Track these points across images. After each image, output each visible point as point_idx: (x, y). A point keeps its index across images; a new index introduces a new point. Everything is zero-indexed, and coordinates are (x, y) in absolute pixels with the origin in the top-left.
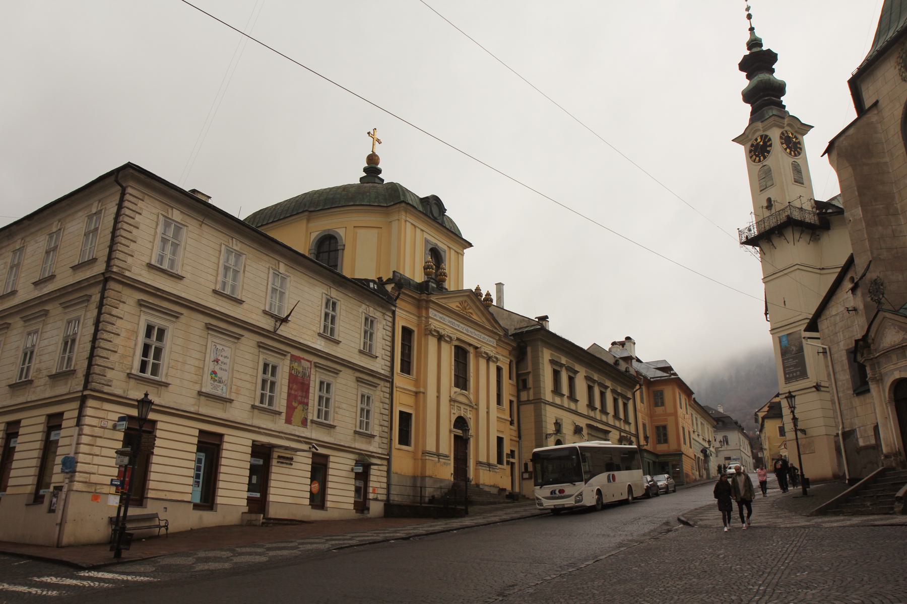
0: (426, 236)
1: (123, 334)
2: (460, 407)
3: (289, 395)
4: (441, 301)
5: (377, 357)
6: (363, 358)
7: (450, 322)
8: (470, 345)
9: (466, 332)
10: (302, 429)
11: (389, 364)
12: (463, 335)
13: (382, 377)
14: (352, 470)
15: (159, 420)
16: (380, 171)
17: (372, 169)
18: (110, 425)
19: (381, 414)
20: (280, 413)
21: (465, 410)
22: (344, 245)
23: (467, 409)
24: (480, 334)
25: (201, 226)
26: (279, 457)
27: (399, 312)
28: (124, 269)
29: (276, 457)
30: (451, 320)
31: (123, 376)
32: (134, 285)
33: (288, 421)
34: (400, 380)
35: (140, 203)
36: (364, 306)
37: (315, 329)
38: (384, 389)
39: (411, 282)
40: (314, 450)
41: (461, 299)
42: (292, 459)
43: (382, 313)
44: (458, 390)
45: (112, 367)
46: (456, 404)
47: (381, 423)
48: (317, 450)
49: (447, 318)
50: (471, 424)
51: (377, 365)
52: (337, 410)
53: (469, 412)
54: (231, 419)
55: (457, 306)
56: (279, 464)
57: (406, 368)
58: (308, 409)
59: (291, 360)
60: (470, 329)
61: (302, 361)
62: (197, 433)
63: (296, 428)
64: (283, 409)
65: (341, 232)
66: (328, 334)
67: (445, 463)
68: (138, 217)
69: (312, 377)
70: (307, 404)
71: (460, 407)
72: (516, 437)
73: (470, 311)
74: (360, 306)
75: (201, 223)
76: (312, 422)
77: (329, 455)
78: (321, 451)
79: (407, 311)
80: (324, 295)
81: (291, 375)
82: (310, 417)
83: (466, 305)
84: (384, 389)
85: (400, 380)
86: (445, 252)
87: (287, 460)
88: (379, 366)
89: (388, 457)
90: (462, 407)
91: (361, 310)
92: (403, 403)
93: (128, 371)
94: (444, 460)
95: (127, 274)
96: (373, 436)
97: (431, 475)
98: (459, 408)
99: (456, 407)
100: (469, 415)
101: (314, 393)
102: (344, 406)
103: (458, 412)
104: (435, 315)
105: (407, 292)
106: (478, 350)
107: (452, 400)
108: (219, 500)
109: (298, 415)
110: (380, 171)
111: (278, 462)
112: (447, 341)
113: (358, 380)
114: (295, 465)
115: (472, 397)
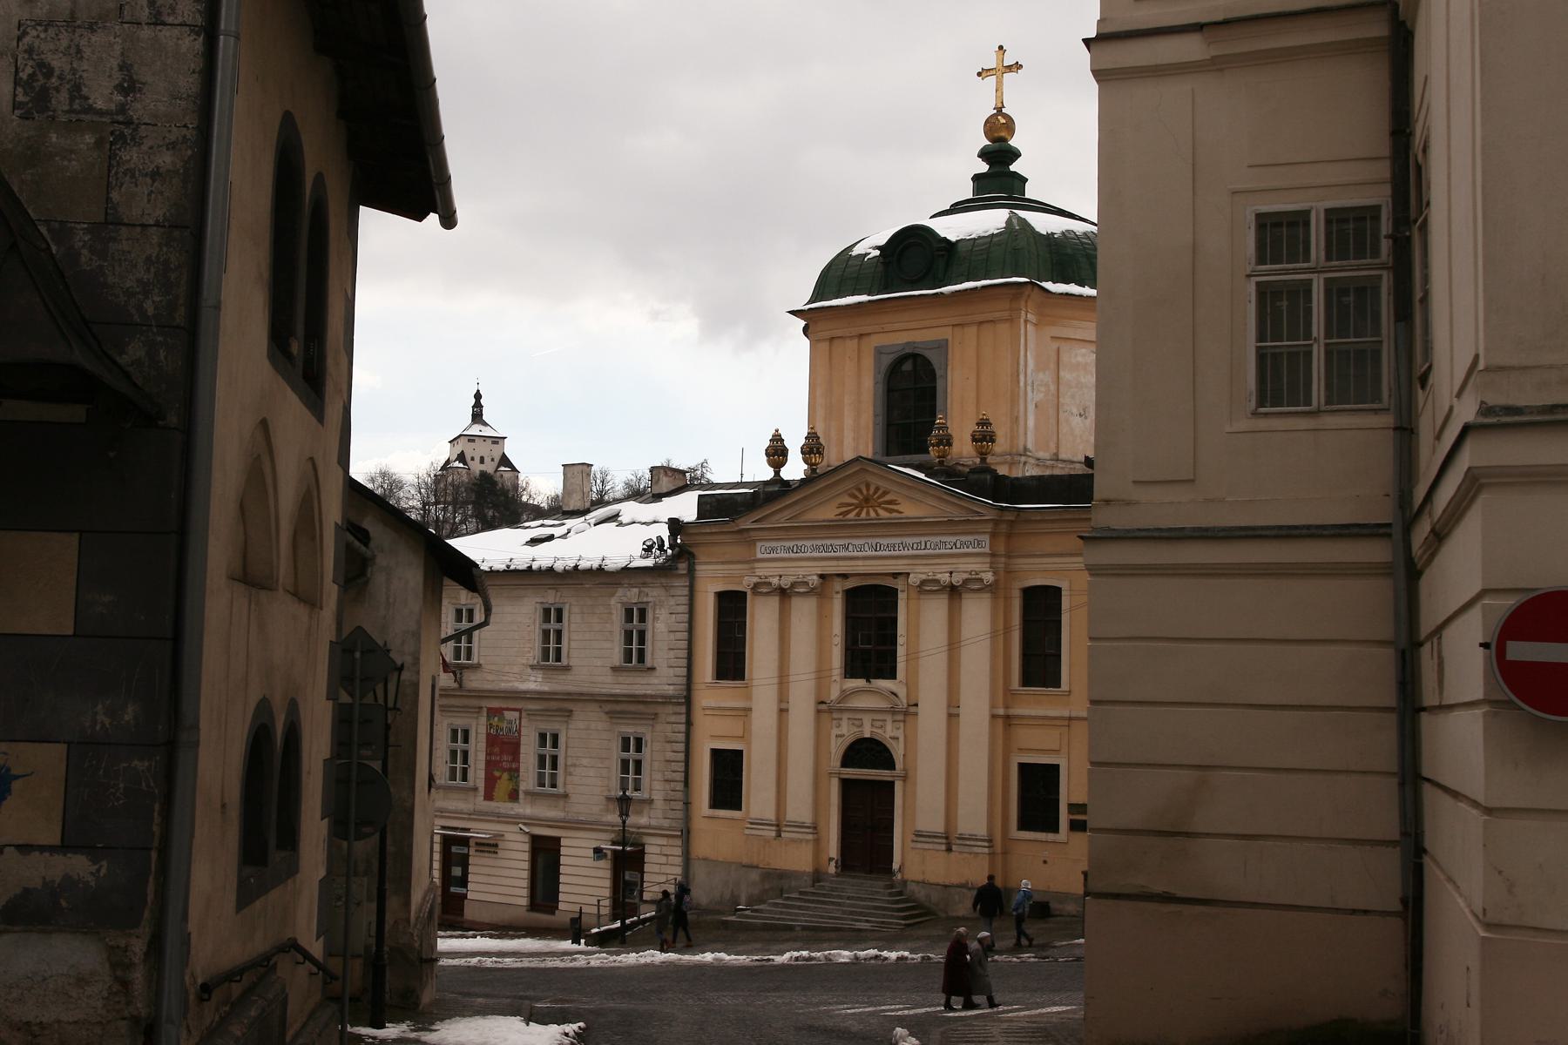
3: (488, 763)
6: (620, 678)
7: (817, 548)
8: (895, 575)
9: (874, 553)
10: (510, 805)
12: (860, 563)
20: (475, 789)
23: (885, 720)
24: (923, 539)
30: (819, 542)
33: (489, 796)
34: (711, 695)
36: (620, 592)
37: (524, 661)
38: (673, 719)
41: (849, 485)
42: (496, 845)
44: (860, 683)
46: (845, 716)
47: (666, 777)
49: (808, 543)
50: (898, 752)
52: (572, 769)
53: (889, 726)
56: (478, 854)
58: (518, 776)
59: (488, 716)
60: (884, 541)
61: (506, 713)
63: (500, 804)
64: (481, 785)
67: (793, 840)
69: (524, 731)
70: (517, 770)
71: (861, 719)
73: (888, 498)
74: (613, 595)
76: (527, 793)
79: (723, 563)
80: (538, 606)
81: (488, 735)
82: (523, 787)
83: (865, 492)
84: (673, 719)
85: (711, 695)
87: (490, 847)
90: (867, 720)
91: (613, 601)
92: (711, 736)
97: (755, 864)
98: (856, 722)
99: (844, 723)
100: (889, 732)
101: (529, 751)
102: (585, 762)
103: (856, 730)
104: (773, 550)
105: (708, 531)
109: (503, 785)
111: (476, 851)
113: (611, 715)
114: (501, 854)
115: (902, 692)
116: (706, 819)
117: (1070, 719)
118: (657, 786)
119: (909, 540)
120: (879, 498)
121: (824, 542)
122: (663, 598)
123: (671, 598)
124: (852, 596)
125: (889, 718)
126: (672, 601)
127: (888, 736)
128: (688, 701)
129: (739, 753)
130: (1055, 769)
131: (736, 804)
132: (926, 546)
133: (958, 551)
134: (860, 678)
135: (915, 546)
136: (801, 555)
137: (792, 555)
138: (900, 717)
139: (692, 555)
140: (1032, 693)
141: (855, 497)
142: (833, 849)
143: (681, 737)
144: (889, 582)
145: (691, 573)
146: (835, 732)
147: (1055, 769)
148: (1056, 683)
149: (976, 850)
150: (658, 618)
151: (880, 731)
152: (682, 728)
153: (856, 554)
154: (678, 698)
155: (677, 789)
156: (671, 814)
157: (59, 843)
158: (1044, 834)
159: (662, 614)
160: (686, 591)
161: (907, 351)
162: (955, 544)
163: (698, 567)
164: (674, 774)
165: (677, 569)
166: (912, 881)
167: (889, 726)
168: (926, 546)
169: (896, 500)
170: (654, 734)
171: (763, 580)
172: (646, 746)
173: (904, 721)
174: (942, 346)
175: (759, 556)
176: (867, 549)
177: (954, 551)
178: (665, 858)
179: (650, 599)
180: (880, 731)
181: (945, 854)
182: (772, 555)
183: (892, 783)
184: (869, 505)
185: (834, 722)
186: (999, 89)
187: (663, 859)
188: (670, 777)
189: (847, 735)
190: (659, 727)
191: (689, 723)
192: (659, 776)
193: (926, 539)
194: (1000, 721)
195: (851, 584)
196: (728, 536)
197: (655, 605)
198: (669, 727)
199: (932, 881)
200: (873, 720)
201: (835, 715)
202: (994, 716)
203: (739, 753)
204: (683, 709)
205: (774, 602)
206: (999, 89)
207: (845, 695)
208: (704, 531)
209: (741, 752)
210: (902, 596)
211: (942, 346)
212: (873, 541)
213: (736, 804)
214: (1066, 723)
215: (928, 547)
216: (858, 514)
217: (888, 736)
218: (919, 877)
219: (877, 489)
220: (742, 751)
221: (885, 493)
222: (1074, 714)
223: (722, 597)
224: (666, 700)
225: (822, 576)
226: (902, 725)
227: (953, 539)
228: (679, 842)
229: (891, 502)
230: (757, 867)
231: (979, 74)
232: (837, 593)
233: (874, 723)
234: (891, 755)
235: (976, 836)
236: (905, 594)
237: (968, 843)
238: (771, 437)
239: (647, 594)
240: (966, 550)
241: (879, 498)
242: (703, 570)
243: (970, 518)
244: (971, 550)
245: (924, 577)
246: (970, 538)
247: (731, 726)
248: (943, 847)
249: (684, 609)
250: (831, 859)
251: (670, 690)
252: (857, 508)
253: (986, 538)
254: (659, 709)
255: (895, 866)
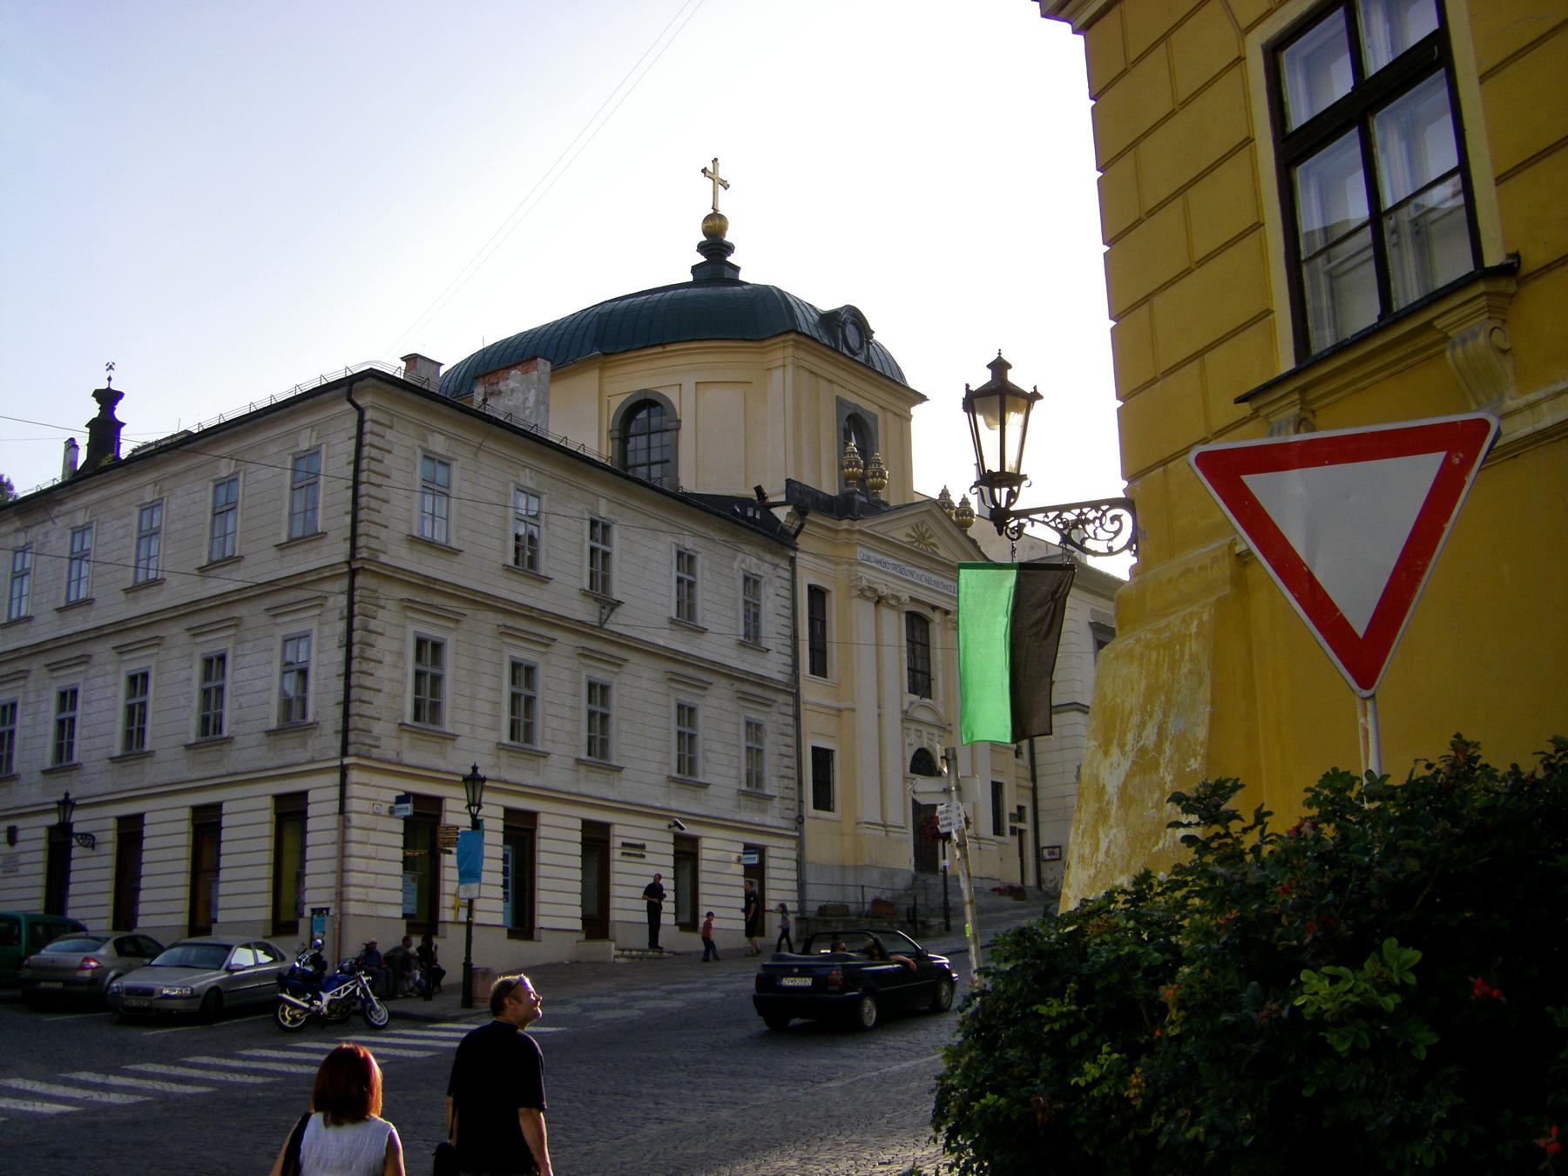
0: (838, 391)
1: (388, 659)
4: (877, 529)
5: (768, 650)
8: (934, 608)
11: (789, 661)
14: (739, 860)
15: (544, 810)
16: (729, 249)
17: (715, 246)
18: (385, 809)
22: (679, 421)
25: (476, 454)
26: (624, 845)
27: (803, 560)
28: (377, 551)
29: (620, 846)
31: (392, 727)
32: (393, 575)
35: (389, 435)
39: (821, 496)
40: (677, 829)
43: (773, 564)
44: (915, 698)
45: (377, 715)
48: (682, 828)
52: (709, 754)
53: (936, 738)
54: (549, 785)
55: (908, 535)
57: (819, 666)
62: (579, 825)
65: (672, 395)
66: (686, 615)
68: (387, 458)
72: (1027, 780)
75: (475, 450)
77: (700, 837)
78: (689, 830)
85: (812, 690)
86: (875, 418)
88: (773, 666)
89: (797, 834)
90: (925, 730)
93: (399, 721)
95: (383, 558)
96: (771, 798)
106: (950, 617)
107: (907, 718)
108: (541, 922)
110: (729, 249)
111: (623, 854)
112: (892, 607)
115: (941, 710)
137: (880, 567)
228: (792, 843)
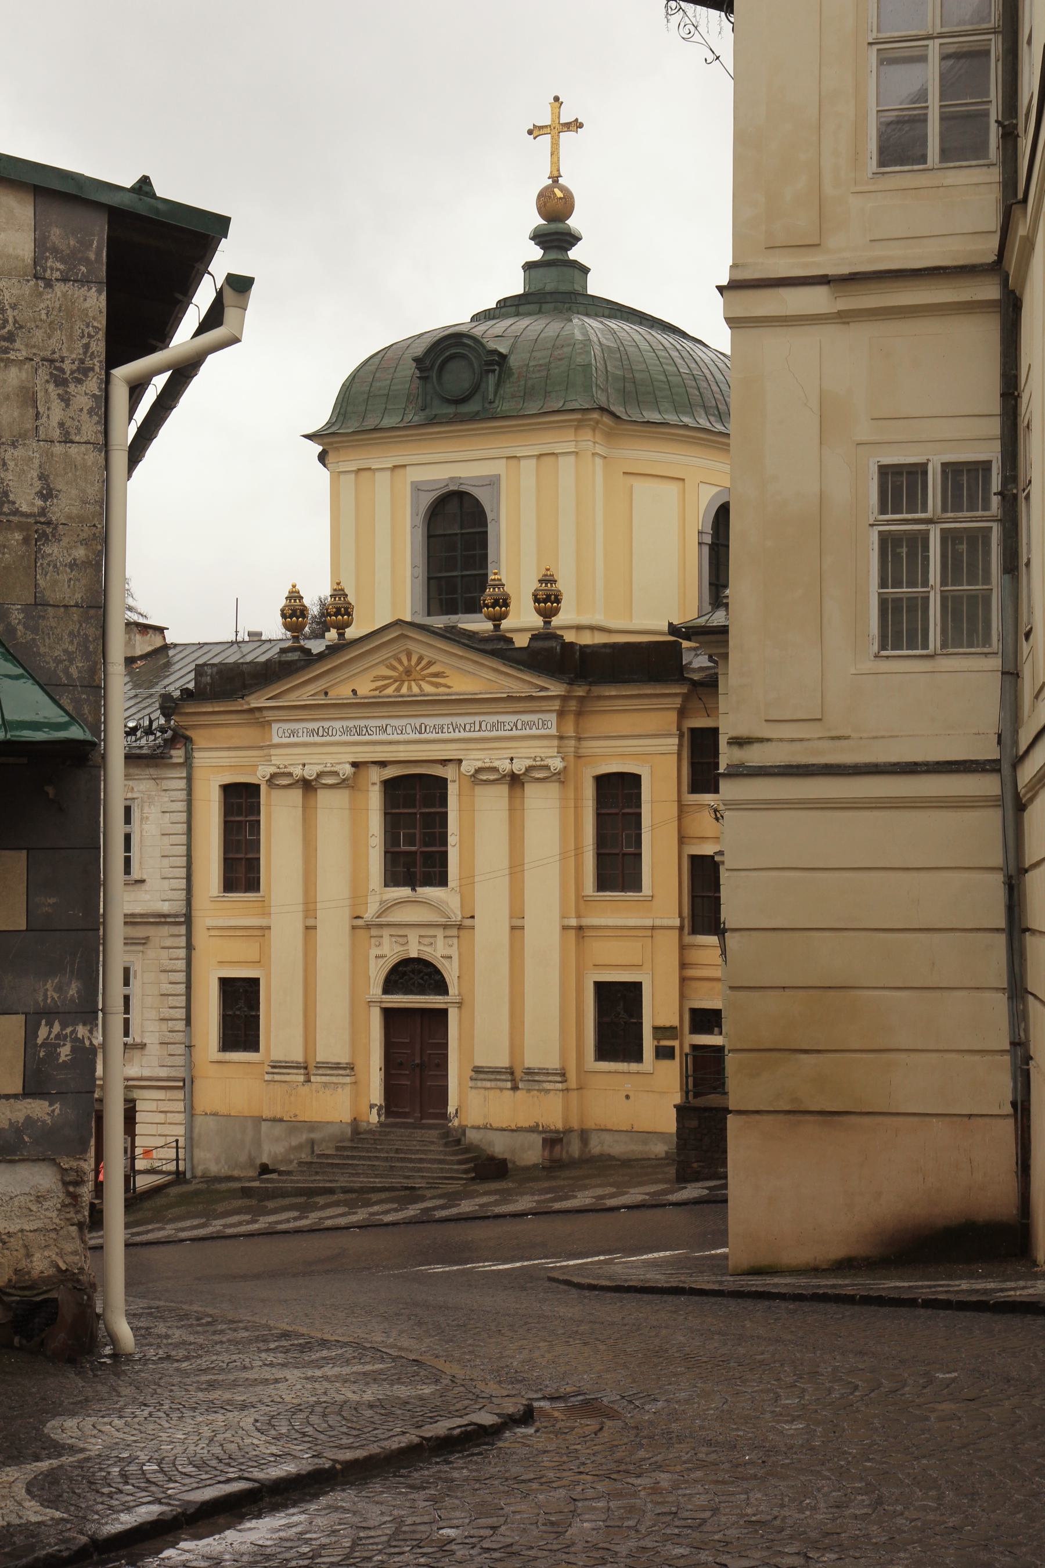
2: (406, 936)
7: (346, 731)
8: (444, 762)
9: (418, 736)
12: (401, 748)
13: (152, 920)
19: (162, 995)
21: (426, 941)
23: (435, 936)
24: (477, 719)
30: (351, 724)
38: (169, 942)
41: (384, 654)
44: (405, 892)
46: (386, 932)
47: (162, 1016)
49: (337, 725)
50: (451, 973)
51: (147, 897)
53: (440, 942)
60: (430, 722)
67: (325, 1085)
71: (406, 936)
73: (433, 669)
79: (229, 749)
84: (169, 942)
90: (413, 936)
94: (324, 1079)
96: (143, 1046)
98: (401, 940)
99: (386, 940)
103: (398, 948)
104: (293, 733)
105: (210, 709)
116: (215, 1066)
117: (653, 928)
118: (152, 1026)
119: (460, 721)
120: (423, 669)
121: (357, 723)
122: (154, 793)
123: (163, 793)
124: (390, 786)
125: (440, 933)
126: (165, 798)
127: (439, 956)
128: (188, 919)
129: (255, 982)
130: (637, 986)
131: (252, 1045)
132: (480, 726)
133: (519, 733)
134: (404, 885)
135: (468, 727)
136: (328, 739)
138: (454, 932)
139: (188, 740)
140: (608, 899)
141: (394, 668)
142: (376, 1093)
143: (181, 965)
144: (438, 771)
145: (188, 763)
146: (374, 952)
147: (637, 986)
148: (637, 886)
149: (547, 1086)
150: (147, 818)
151: (428, 949)
152: (182, 953)
153: (396, 737)
154: (176, 916)
155: (177, 1029)
156: (169, 1061)
157: (21, 1092)
158: (626, 1064)
159: (152, 812)
160: (182, 784)
161: (452, 488)
162: (516, 725)
163: (196, 754)
164: (172, 1011)
165: (171, 757)
166: (473, 1127)
167: (440, 942)
168: (480, 726)
169: (443, 672)
170: (146, 961)
171: (282, 771)
172: (135, 978)
173: (458, 937)
174: (493, 482)
175: (276, 740)
176: (409, 730)
177: (514, 733)
178: (162, 1115)
179: (135, 795)
180: (428, 949)
181: (511, 1092)
182: (292, 740)
183: (443, 1013)
184: (410, 678)
185: (373, 940)
186: (555, 152)
187: (160, 1118)
188: (167, 1016)
189: (388, 956)
190: (151, 953)
191: (190, 947)
192: (153, 1014)
193: (482, 718)
194: (573, 933)
195: (390, 773)
196: (234, 716)
197: (143, 801)
198: (164, 953)
199: (495, 1125)
200: (420, 936)
201: (374, 932)
202: (565, 928)
203: (255, 982)
204: (183, 930)
205: (296, 795)
206: (555, 152)
207: (387, 908)
208: (204, 710)
209: (256, 981)
210: (452, 789)
211: (493, 482)
212: (417, 722)
213: (252, 1045)
214: (649, 933)
215: (484, 728)
216: (398, 689)
217: (439, 956)
218: (480, 1122)
219: (421, 659)
220: (258, 980)
221: (430, 664)
222: (658, 922)
223: (230, 791)
224: (161, 919)
225: (355, 765)
226: (455, 940)
227: (513, 718)
229: (436, 675)
230: (281, 1120)
231: (530, 132)
232: (374, 784)
233: (422, 940)
234: (443, 976)
235: (547, 1069)
236: (456, 785)
237: (537, 1078)
238: (287, 594)
239: (133, 788)
240: (528, 732)
241: (423, 669)
242: (201, 758)
243: (534, 694)
244: (534, 732)
245: (479, 764)
246: (534, 717)
247: (247, 950)
248: (509, 1085)
249: (182, 806)
250: (372, 1106)
251: (165, 908)
252: (396, 681)
253: (553, 717)
254: (150, 931)
255: (451, 1109)
